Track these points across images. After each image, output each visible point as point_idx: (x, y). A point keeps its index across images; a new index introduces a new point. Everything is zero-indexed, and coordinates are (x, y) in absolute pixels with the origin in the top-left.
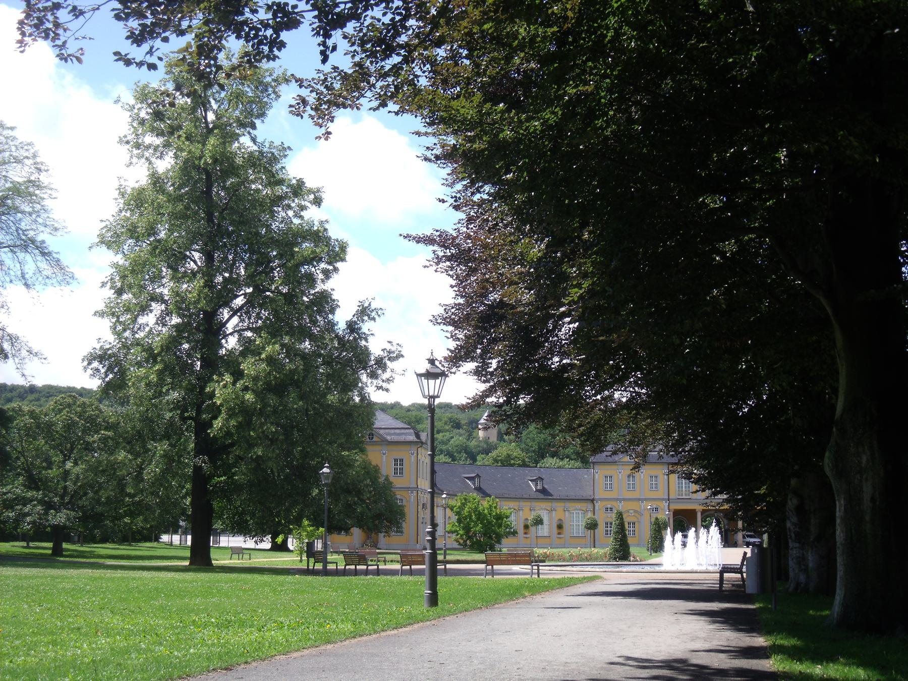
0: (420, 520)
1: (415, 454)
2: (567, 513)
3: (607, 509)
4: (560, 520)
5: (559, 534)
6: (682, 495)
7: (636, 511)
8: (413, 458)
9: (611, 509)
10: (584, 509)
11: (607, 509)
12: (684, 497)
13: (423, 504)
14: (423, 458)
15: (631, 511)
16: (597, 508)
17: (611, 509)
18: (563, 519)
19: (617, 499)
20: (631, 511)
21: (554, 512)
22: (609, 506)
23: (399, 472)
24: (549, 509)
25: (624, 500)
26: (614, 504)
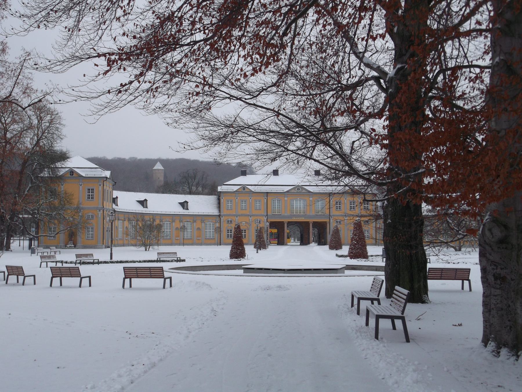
1: (102, 185)
2: (203, 224)
3: (228, 221)
6: (275, 213)
7: (246, 223)
8: (100, 188)
9: (231, 221)
11: (228, 221)
12: (277, 214)
14: (108, 188)
15: (243, 223)
16: (222, 220)
17: (231, 221)
18: (200, 227)
19: (234, 215)
21: (195, 224)
22: (230, 220)
23: (90, 197)
25: (239, 215)
26: (234, 218)
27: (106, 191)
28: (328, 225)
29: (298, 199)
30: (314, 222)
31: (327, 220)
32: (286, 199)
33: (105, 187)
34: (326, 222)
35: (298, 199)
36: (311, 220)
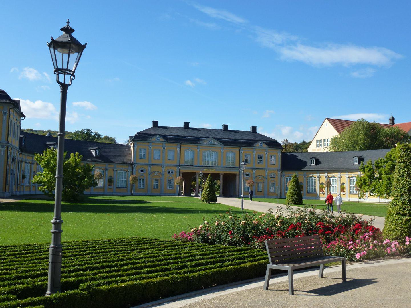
0: (9, 172)
1: (7, 114)
3: (141, 171)
4: (111, 176)
5: (109, 185)
7: (159, 173)
8: (5, 117)
9: (143, 171)
10: (126, 170)
11: (141, 171)
13: (13, 159)
16: (134, 170)
17: (143, 171)
20: (157, 172)
21: (107, 172)
22: (142, 169)
24: (104, 169)
25: (152, 165)
26: (146, 167)
27: (13, 124)
28: (237, 177)
29: (210, 151)
30: (224, 174)
31: (238, 173)
32: (198, 150)
33: (11, 117)
34: (234, 175)
35: (210, 151)
36: (222, 172)
